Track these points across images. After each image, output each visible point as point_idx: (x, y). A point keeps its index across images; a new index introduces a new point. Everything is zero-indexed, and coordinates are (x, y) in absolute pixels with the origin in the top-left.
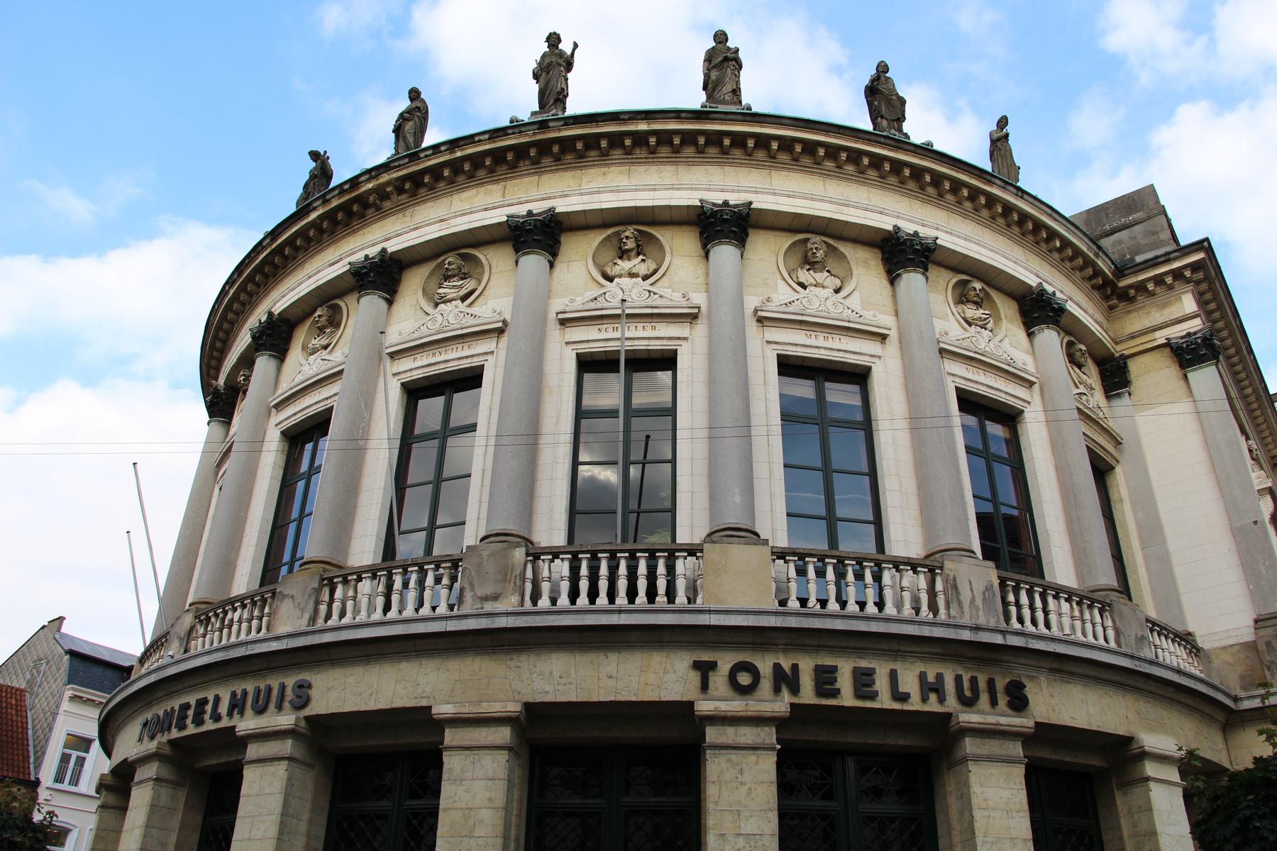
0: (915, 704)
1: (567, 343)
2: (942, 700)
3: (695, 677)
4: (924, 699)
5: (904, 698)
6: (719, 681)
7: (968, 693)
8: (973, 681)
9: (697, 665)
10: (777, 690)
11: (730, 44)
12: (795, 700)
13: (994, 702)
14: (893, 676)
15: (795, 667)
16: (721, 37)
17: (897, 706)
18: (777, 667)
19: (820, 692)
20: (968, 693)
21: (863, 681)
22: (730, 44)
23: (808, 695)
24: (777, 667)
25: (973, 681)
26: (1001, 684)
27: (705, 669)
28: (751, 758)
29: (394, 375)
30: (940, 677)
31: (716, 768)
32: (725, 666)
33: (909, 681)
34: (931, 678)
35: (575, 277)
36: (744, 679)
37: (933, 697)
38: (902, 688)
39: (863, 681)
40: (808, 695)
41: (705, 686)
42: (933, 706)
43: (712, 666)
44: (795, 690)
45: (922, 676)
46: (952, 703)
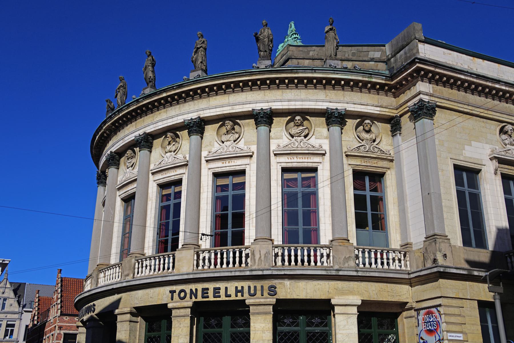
0: (233, 298)
4: (236, 296)
5: (230, 296)
6: (176, 295)
7: (252, 292)
8: (255, 287)
9: (170, 292)
12: (196, 300)
17: (227, 299)
18: (191, 290)
20: (252, 292)
21: (217, 290)
24: (191, 290)
25: (255, 287)
26: (266, 288)
28: (183, 319)
30: (242, 287)
31: (175, 323)
33: (232, 291)
34: (239, 288)
40: (200, 299)
42: (240, 297)
45: (236, 288)
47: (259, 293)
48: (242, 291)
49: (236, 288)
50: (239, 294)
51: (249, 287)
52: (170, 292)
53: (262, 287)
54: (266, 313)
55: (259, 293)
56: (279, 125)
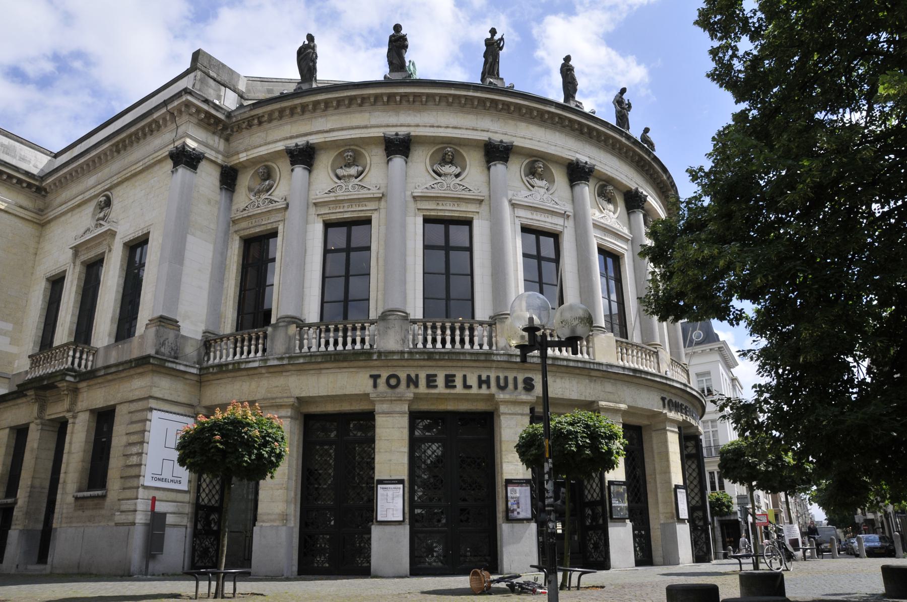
0: (475, 390)
1: (318, 215)
2: (489, 387)
3: (371, 382)
4: (480, 387)
5: (470, 387)
6: (382, 382)
7: (502, 383)
9: (371, 376)
10: (408, 386)
11: (403, 32)
12: (417, 391)
13: (516, 387)
14: (465, 377)
15: (417, 376)
16: (397, 28)
18: (409, 376)
19: (429, 386)
20: (502, 383)
22: (403, 32)
23: (422, 388)
24: (409, 376)
25: (506, 378)
27: (375, 378)
29: (236, 232)
30: (488, 377)
32: (385, 375)
35: (323, 180)
36: (393, 382)
37: (484, 386)
38: (469, 383)
39: (449, 381)
41: (375, 386)
42: (484, 390)
43: (379, 376)
44: (416, 385)
45: (480, 377)
46: (494, 389)
47: (511, 386)
48: (488, 382)
49: (480, 377)
50: (484, 386)
51: (498, 378)
52: (371, 376)
53: (515, 379)
54: (522, 415)
55: (511, 386)
56: (421, 160)
